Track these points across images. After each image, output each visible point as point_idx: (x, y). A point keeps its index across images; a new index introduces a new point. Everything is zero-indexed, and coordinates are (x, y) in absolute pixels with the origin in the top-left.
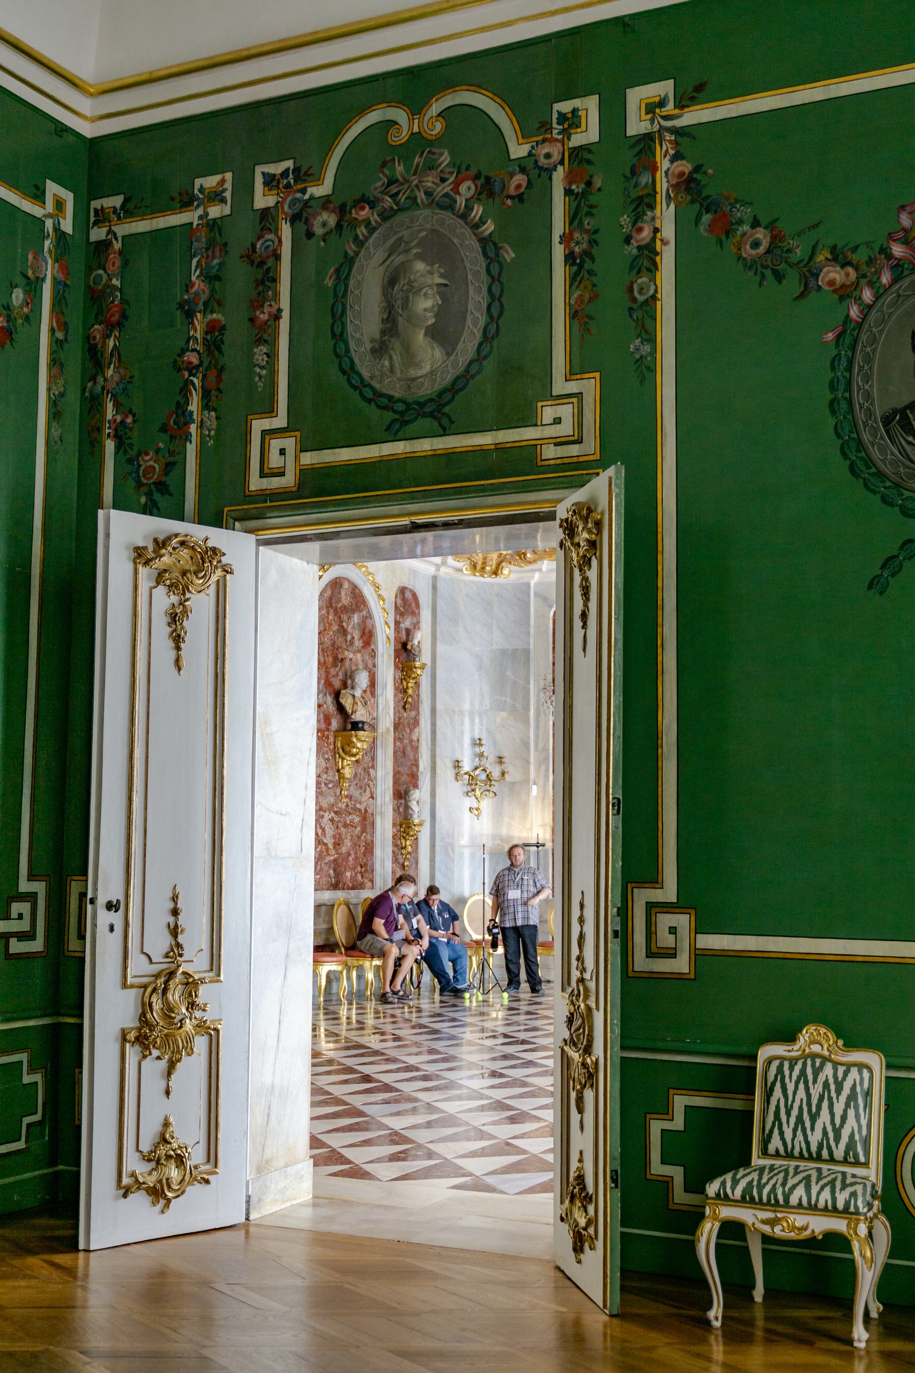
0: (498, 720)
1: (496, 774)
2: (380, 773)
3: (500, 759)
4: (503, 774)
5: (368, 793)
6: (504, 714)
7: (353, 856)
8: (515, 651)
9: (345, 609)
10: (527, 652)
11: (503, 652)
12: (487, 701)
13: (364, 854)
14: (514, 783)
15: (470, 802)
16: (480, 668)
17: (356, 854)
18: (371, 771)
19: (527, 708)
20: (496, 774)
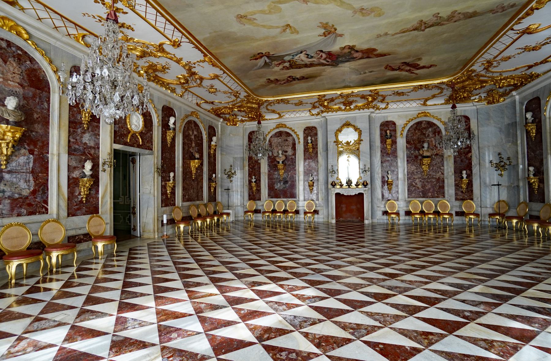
0: (508, 146)
1: (508, 163)
2: (446, 167)
3: (509, 159)
4: (510, 162)
5: (440, 173)
6: (510, 144)
7: (432, 189)
8: (512, 123)
9: (424, 128)
10: (516, 122)
11: (509, 124)
12: (504, 141)
13: (439, 189)
14: (514, 165)
15: (499, 172)
16: (500, 131)
17: (434, 189)
18: (442, 168)
19: (517, 141)
20: (508, 163)
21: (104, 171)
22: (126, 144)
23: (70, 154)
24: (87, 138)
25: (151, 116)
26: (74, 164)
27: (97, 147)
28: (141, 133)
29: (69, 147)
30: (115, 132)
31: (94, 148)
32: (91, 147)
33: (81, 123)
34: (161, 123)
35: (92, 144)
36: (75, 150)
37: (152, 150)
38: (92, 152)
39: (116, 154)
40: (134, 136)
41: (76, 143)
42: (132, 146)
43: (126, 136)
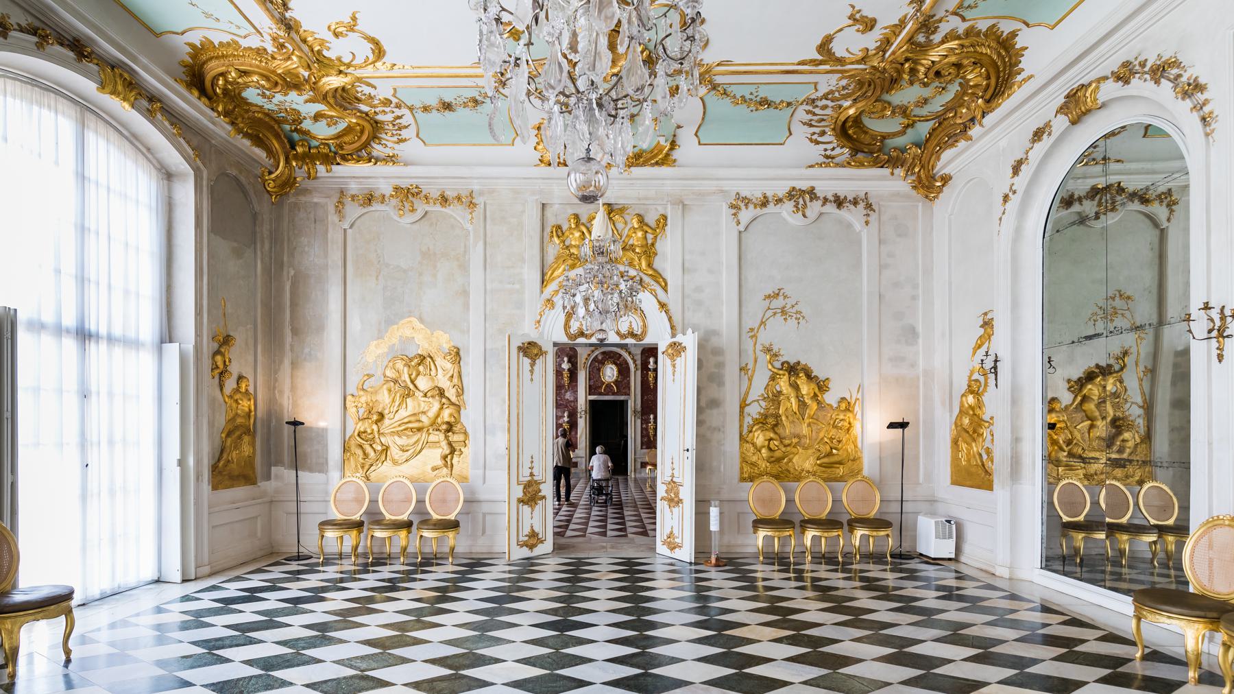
21: (581, 417)
22: (600, 394)
23: (557, 408)
24: (568, 396)
25: (628, 364)
26: (560, 414)
27: (576, 400)
28: (616, 382)
29: (556, 403)
30: (590, 386)
31: (573, 401)
32: (571, 401)
33: (564, 386)
34: (639, 367)
35: (572, 399)
36: (561, 405)
37: (629, 395)
38: (572, 404)
39: (593, 404)
40: (609, 386)
41: (561, 400)
42: (607, 394)
43: (601, 387)
